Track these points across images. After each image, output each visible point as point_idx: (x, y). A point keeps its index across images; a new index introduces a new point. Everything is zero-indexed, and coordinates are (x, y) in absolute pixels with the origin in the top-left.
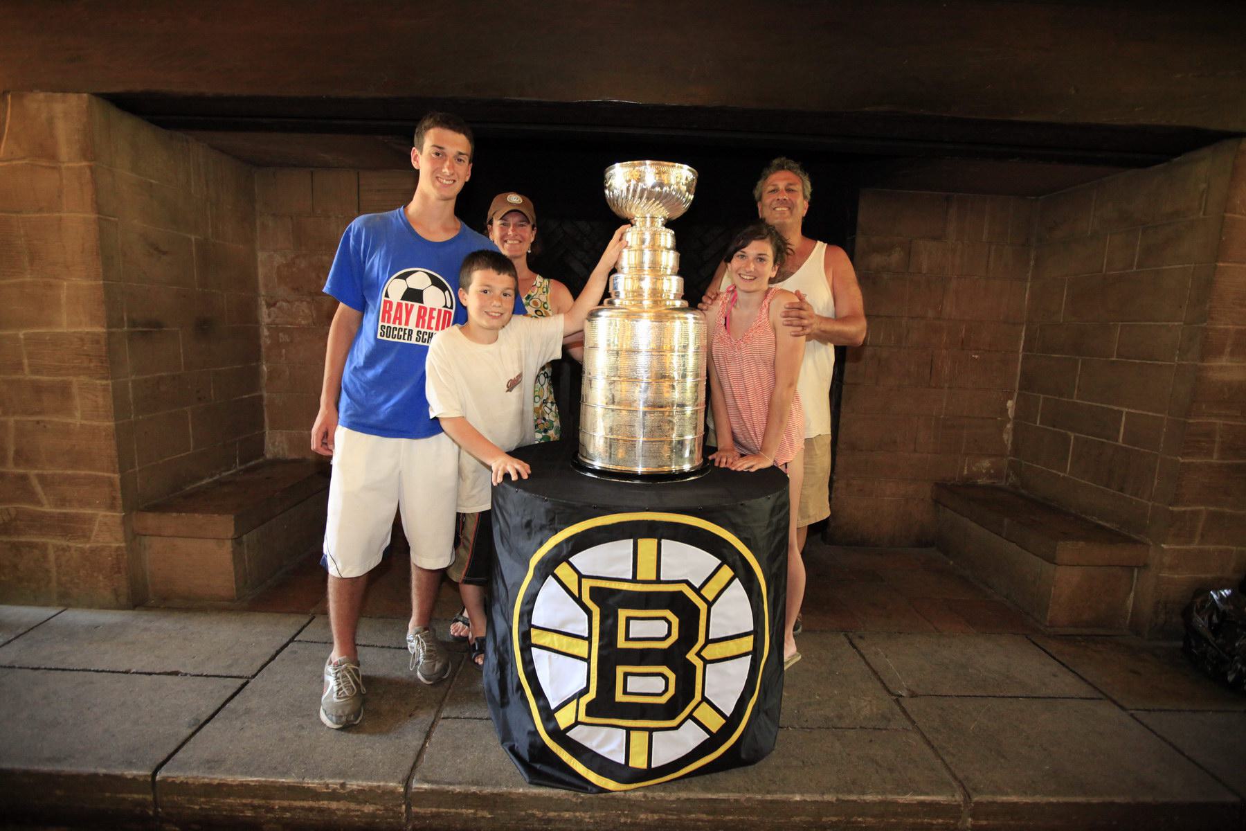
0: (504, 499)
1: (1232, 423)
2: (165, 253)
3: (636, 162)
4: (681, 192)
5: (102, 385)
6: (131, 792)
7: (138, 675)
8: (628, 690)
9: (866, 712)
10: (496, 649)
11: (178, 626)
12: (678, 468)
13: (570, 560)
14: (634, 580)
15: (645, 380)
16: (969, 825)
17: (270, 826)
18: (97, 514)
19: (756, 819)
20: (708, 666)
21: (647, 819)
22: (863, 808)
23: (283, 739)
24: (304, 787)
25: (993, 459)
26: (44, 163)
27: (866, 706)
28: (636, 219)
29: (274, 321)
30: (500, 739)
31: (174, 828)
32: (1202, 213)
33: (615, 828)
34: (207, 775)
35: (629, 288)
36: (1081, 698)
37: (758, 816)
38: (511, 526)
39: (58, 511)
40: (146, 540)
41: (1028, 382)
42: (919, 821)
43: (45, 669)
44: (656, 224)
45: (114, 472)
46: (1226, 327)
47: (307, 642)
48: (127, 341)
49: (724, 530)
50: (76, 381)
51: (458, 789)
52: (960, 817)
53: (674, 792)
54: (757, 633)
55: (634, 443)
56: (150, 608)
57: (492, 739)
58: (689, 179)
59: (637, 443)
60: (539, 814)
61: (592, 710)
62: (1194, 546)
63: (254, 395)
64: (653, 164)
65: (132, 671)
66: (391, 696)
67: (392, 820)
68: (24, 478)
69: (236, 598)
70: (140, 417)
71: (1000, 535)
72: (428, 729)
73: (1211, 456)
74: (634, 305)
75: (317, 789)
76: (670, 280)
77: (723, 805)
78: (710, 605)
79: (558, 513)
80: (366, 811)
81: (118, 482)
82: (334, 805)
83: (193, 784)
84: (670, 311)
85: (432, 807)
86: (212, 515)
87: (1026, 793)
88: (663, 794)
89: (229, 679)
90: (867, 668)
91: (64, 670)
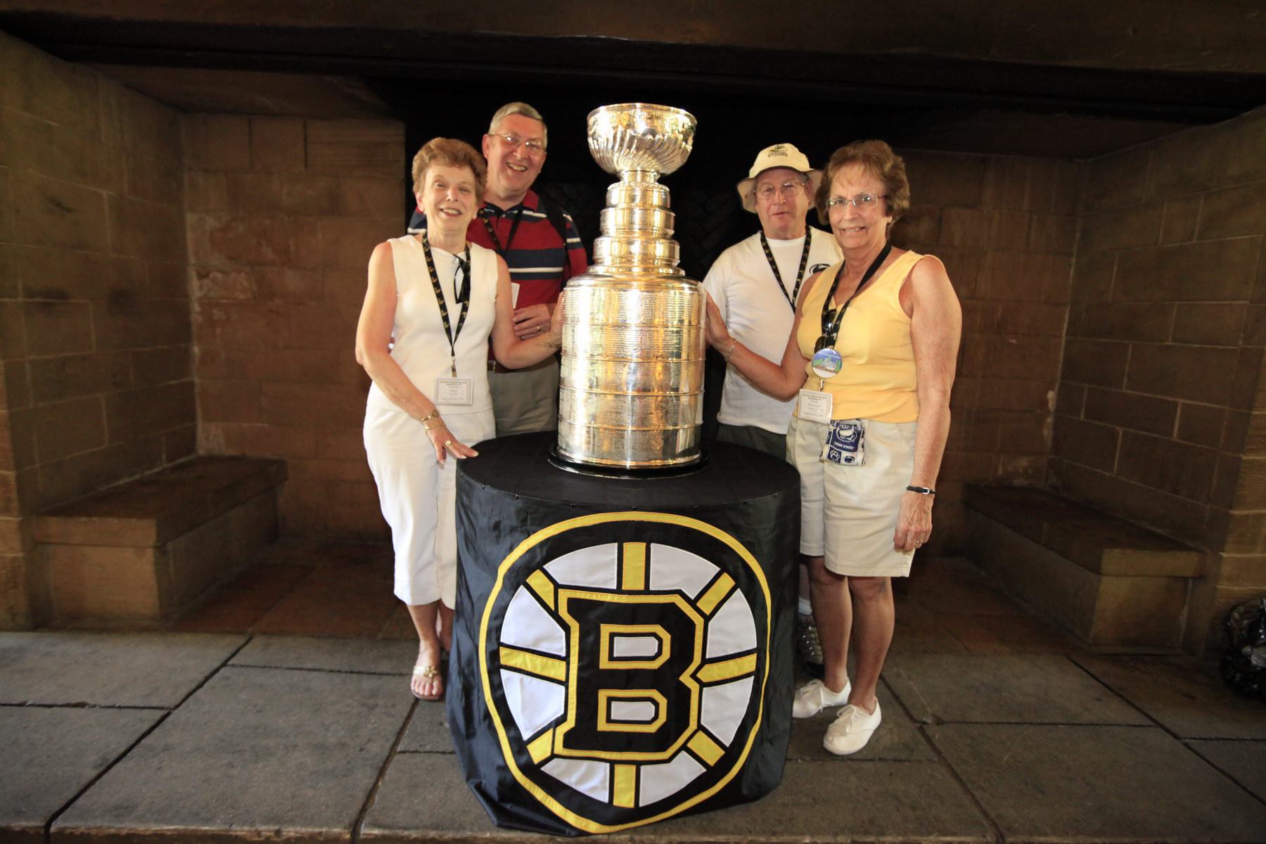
0: (468, 496)
2: (69, 210)
3: (624, 105)
4: (677, 139)
7: (35, 708)
10: (461, 672)
13: (545, 567)
14: (619, 591)
15: (635, 359)
20: (705, 689)
24: (232, 835)
28: (623, 172)
34: (112, 824)
35: (616, 253)
38: (477, 530)
44: (648, 180)
45: (9, 470)
47: (242, 666)
49: (724, 533)
51: (414, 834)
54: (759, 651)
55: (621, 433)
57: (457, 775)
58: (686, 126)
59: (626, 433)
61: (570, 741)
63: (184, 380)
64: (644, 107)
65: (28, 704)
70: (41, 405)
74: (622, 273)
75: (249, 840)
78: (707, 619)
79: (531, 513)
83: (96, 835)
84: (663, 280)
87: (1067, 833)
88: (652, 837)
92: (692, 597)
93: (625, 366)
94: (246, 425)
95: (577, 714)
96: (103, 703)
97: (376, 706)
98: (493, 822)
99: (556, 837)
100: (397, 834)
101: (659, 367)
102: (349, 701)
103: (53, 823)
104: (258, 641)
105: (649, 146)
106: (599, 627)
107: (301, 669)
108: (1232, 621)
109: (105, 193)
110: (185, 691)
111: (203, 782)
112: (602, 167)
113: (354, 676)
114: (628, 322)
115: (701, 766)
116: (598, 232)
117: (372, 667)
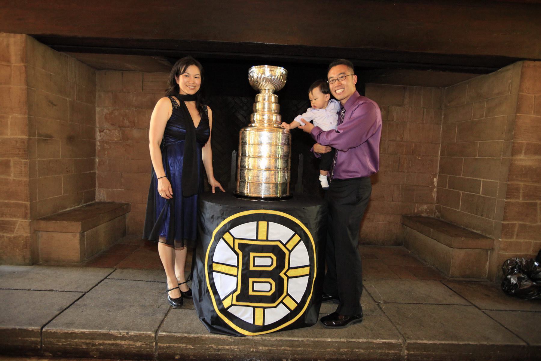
1: (527, 184)
2: (55, 105)
3: (261, 66)
5: (24, 162)
6: (31, 337)
8: (255, 289)
10: (198, 276)
11: (53, 272)
13: (230, 231)
14: (257, 240)
16: (405, 354)
17: (94, 353)
18: (18, 221)
19: (311, 349)
20: (289, 279)
21: (263, 349)
22: (359, 345)
25: (429, 205)
26: (4, 63)
27: (364, 307)
29: (102, 138)
30: (198, 316)
31: (49, 354)
32: (510, 93)
33: (248, 354)
35: (258, 119)
36: (461, 305)
37: (311, 348)
40: (40, 234)
41: (443, 169)
42: (383, 351)
44: (270, 92)
45: (27, 201)
46: (522, 141)
48: (37, 142)
50: (12, 160)
51: (179, 335)
52: (402, 350)
53: (275, 337)
54: (311, 266)
56: (40, 265)
60: (215, 347)
61: (238, 299)
62: (514, 240)
65: (32, 289)
66: (151, 300)
67: (149, 350)
69: (80, 261)
70: (41, 177)
71: (429, 237)
72: (166, 312)
73: (519, 199)
75: (116, 335)
77: (296, 343)
78: (290, 252)
80: (137, 345)
81: (29, 205)
82: (123, 342)
83: (60, 333)
86: (71, 222)
87: (431, 339)
88: (270, 338)
89: (76, 293)
90: (366, 292)
92: (284, 243)
93: (261, 159)
94: (115, 190)
95: (241, 288)
96: (59, 291)
99: (233, 337)
100: (172, 335)
102: (154, 291)
103: (44, 328)
104: (118, 271)
105: (270, 81)
107: (136, 280)
108: (505, 266)
114: (262, 142)
117: (163, 280)
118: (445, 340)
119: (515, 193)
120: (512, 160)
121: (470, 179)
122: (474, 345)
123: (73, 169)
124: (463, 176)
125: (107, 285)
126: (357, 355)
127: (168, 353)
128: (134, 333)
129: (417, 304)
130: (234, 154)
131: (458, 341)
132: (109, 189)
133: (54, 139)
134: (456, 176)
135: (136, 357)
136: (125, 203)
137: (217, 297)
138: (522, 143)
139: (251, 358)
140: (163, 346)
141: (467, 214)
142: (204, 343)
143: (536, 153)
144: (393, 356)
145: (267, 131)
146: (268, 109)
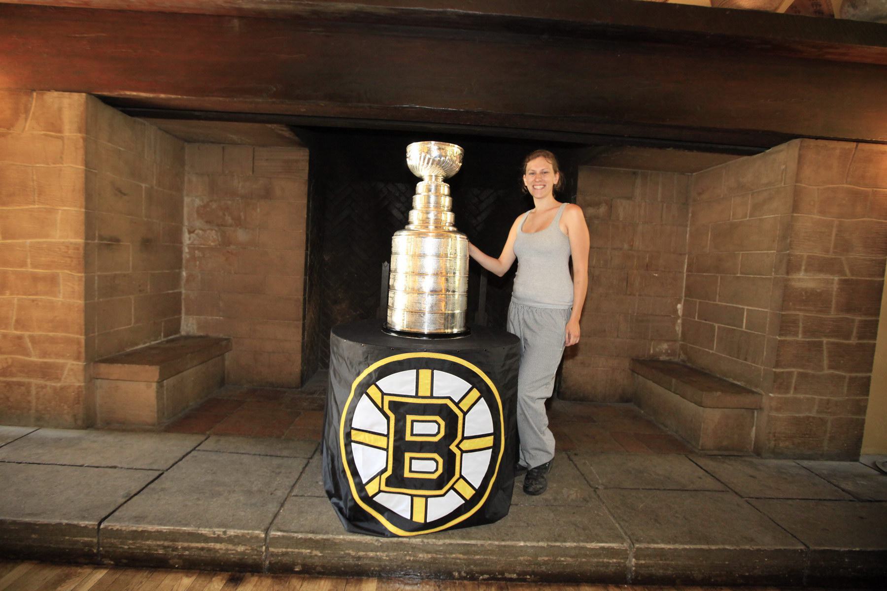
1: (807, 314)
2: (125, 194)
3: (425, 142)
4: (453, 162)
6: (83, 536)
7: (89, 468)
8: (413, 469)
9: (573, 497)
12: (449, 331)
13: (377, 383)
14: (417, 396)
16: (633, 563)
19: (495, 558)
20: (464, 454)
21: (424, 557)
22: (565, 552)
23: (186, 506)
24: (198, 533)
25: (670, 343)
27: (573, 494)
29: (193, 242)
32: (783, 183)
33: (402, 564)
35: (421, 218)
36: (715, 491)
37: (496, 556)
39: (41, 360)
40: (98, 382)
41: (690, 292)
43: (26, 463)
45: (81, 335)
46: (802, 254)
50: (62, 273)
51: (300, 536)
52: (627, 558)
53: (442, 539)
54: (496, 434)
56: (98, 429)
58: (458, 153)
60: (353, 553)
61: (389, 482)
62: (791, 395)
64: (438, 144)
65: (85, 465)
68: (20, 338)
70: (101, 300)
71: (671, 391)
72: (282, 502)
73: (798, 336)
75: (207, 535)
76: (446, 214)
77: (473, 548)
78: (465, 414)
80: (239, 550)
81: (83, 341)
82: (218, 546)
83: (125, 530)
85: (283, 548)
87: (669, 543)
88: (434, 540)
90: (578, 472)
91: (39, 464)
92: (457, 402)
93: (424, 278)
94: (210, 318)
95: (393, 467)
96: (126, 467)
97: (279, 473)
98: (345, 529)
101: (443, 278)
102: (265, 470)
104: (213, 439)
106: (405, 417)
107: (237, 453)
109: (144, 185)
110: (171, 462)
111: (183, 506)
112: (415, 174)
113: (268, 457)
115: (462, 500)
116: (410, 207)
118: (691, 543)
119: (792, 328)
120: (789, 280)
121: (730, 306)
122: (732, 550)
123: (149, 287)
124: (719, 301)
125: (196, 460)
126: (562, 566)
127: (283, 561)
128: (234, 532)
129: (651, 489)
130: (385, 267)
131: (709, 545)
132: (201, 317)
133: (121, 243)
134: (710, 302)
135: (237, 569)
136: (224, 337)
137: (357, 480)
138: (802, 256)
139: (406, 570)
140: (276, 551)
141: (724, 357)
142: (337, 547)
143: (821, 270)
144: (615, 568)
145: (433, 236)
146: (436, 205)
